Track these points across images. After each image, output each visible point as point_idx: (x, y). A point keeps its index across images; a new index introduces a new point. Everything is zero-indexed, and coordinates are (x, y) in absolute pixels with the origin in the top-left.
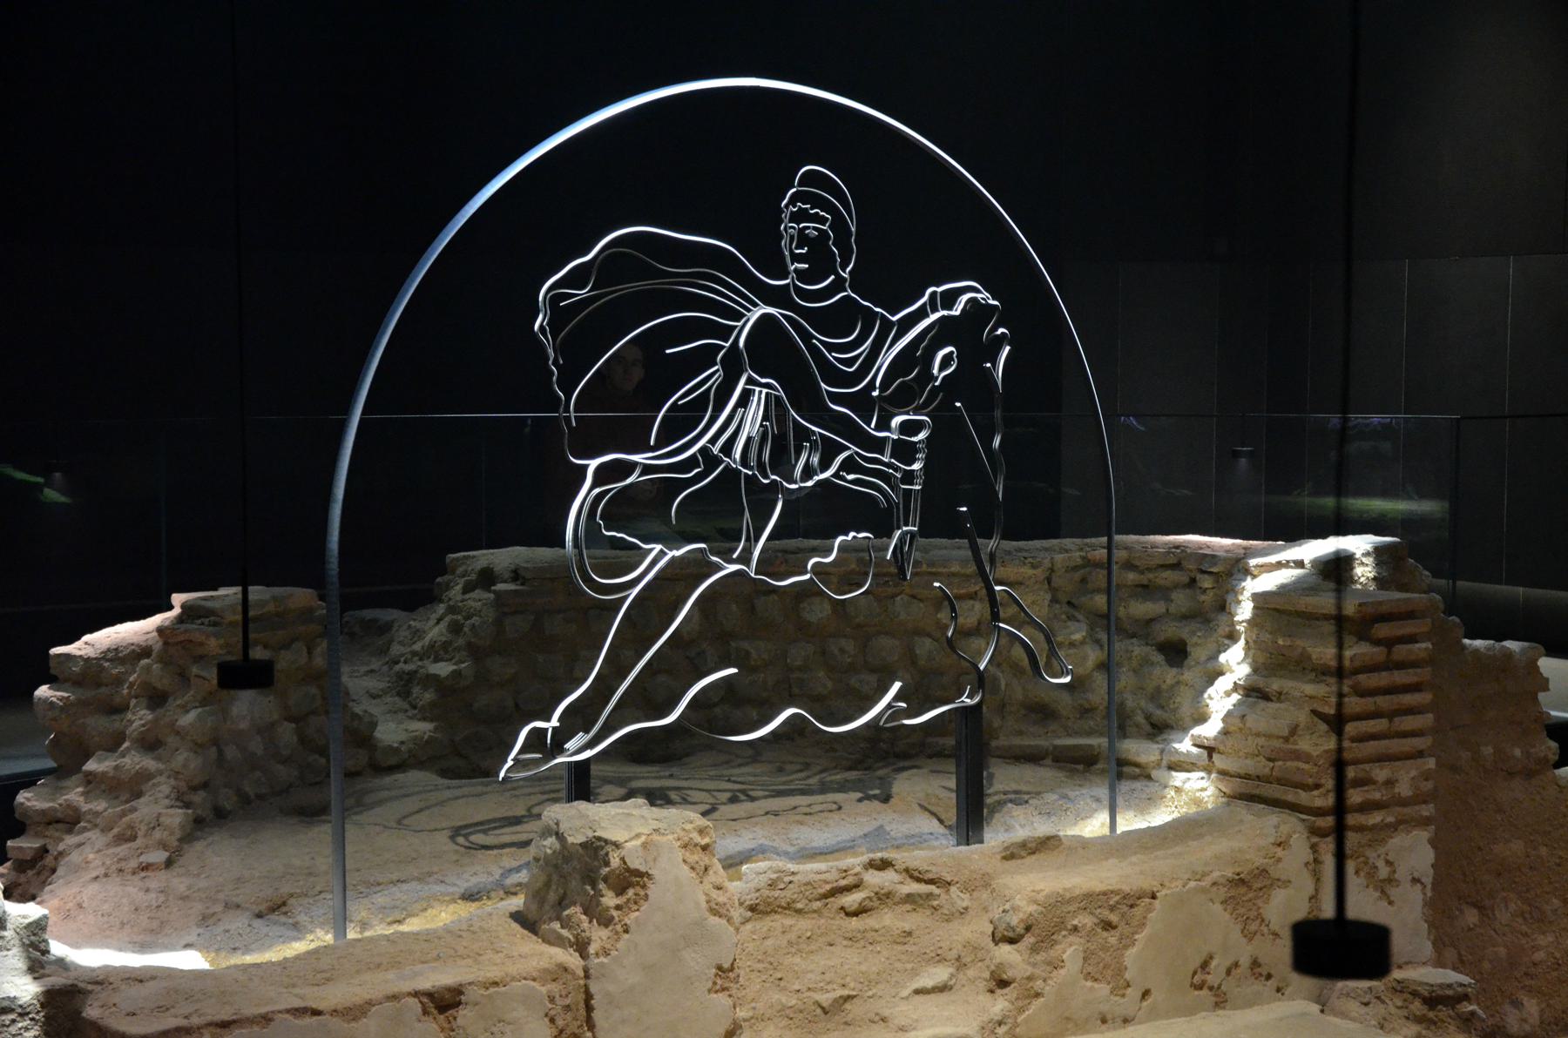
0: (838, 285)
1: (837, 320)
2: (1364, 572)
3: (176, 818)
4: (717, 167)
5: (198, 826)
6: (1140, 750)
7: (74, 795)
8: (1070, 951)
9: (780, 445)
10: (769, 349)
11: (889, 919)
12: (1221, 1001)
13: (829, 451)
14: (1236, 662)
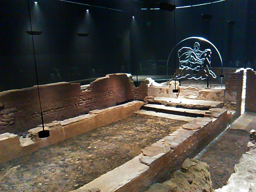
0: (198, 50)
4: (191, 43)
8: (202, 95)
11: (195, 91)
12: (215, 101)
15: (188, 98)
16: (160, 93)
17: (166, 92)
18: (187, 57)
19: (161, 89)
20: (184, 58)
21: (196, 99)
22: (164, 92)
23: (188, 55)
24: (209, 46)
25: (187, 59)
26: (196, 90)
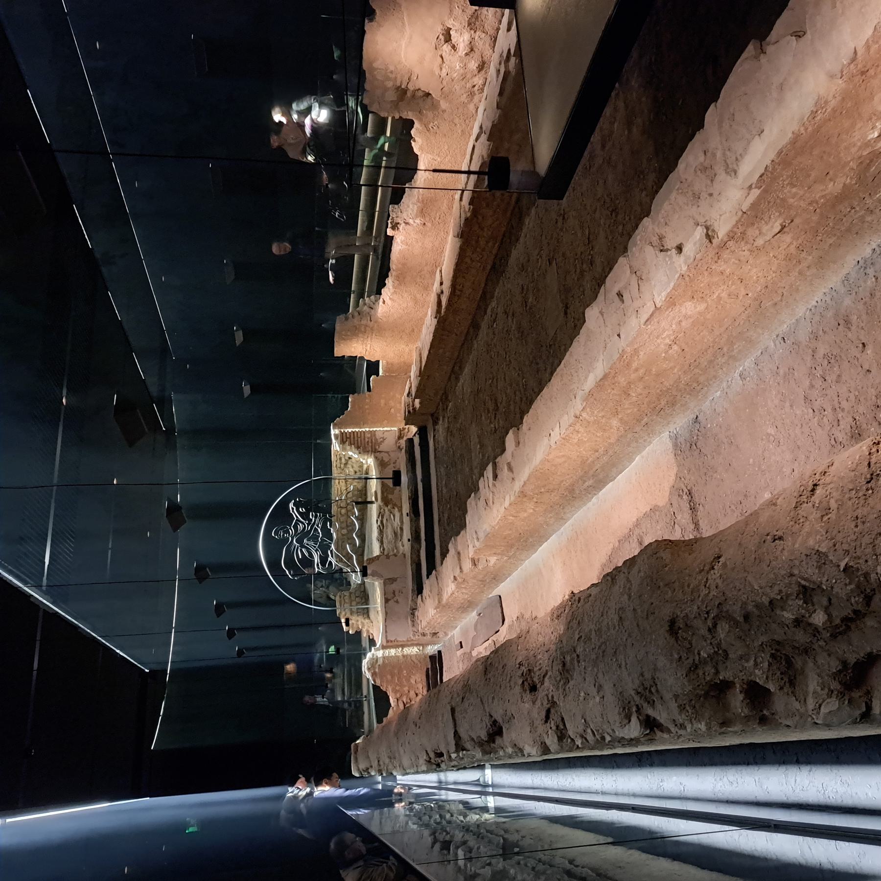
1: (296, 527)
2: (337, 431)
3: (367, 621)
5: (368, 617)
6: (365, 466)
7: (364, 630)
8: (390, 496)
9: (315, 538)
10: (300, 541)
11: (385, 521)
13: (316, 530)
14: (350, 453)
15: (402, 529)
16: (397, 602)
17: (394, 586)
18: (307, 554)
19: (387, 600)
20: (308, 562)
21: (400, 510)
22: (394, 593)
23: (301, 551)
24: (284, 504)
25: (311, 555)
26: (382, 522)
